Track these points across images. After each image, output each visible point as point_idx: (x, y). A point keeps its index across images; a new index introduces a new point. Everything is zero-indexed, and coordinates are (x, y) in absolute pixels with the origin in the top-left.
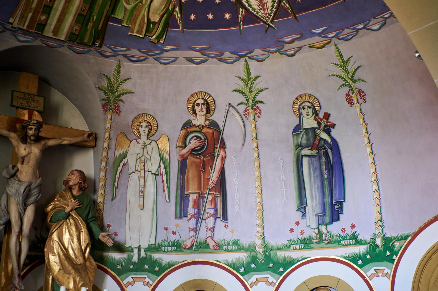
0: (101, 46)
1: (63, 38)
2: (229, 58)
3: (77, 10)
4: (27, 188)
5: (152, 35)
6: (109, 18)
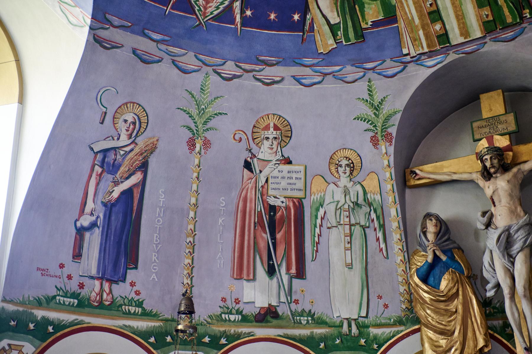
1: (479, 34)
4: (503, 235)
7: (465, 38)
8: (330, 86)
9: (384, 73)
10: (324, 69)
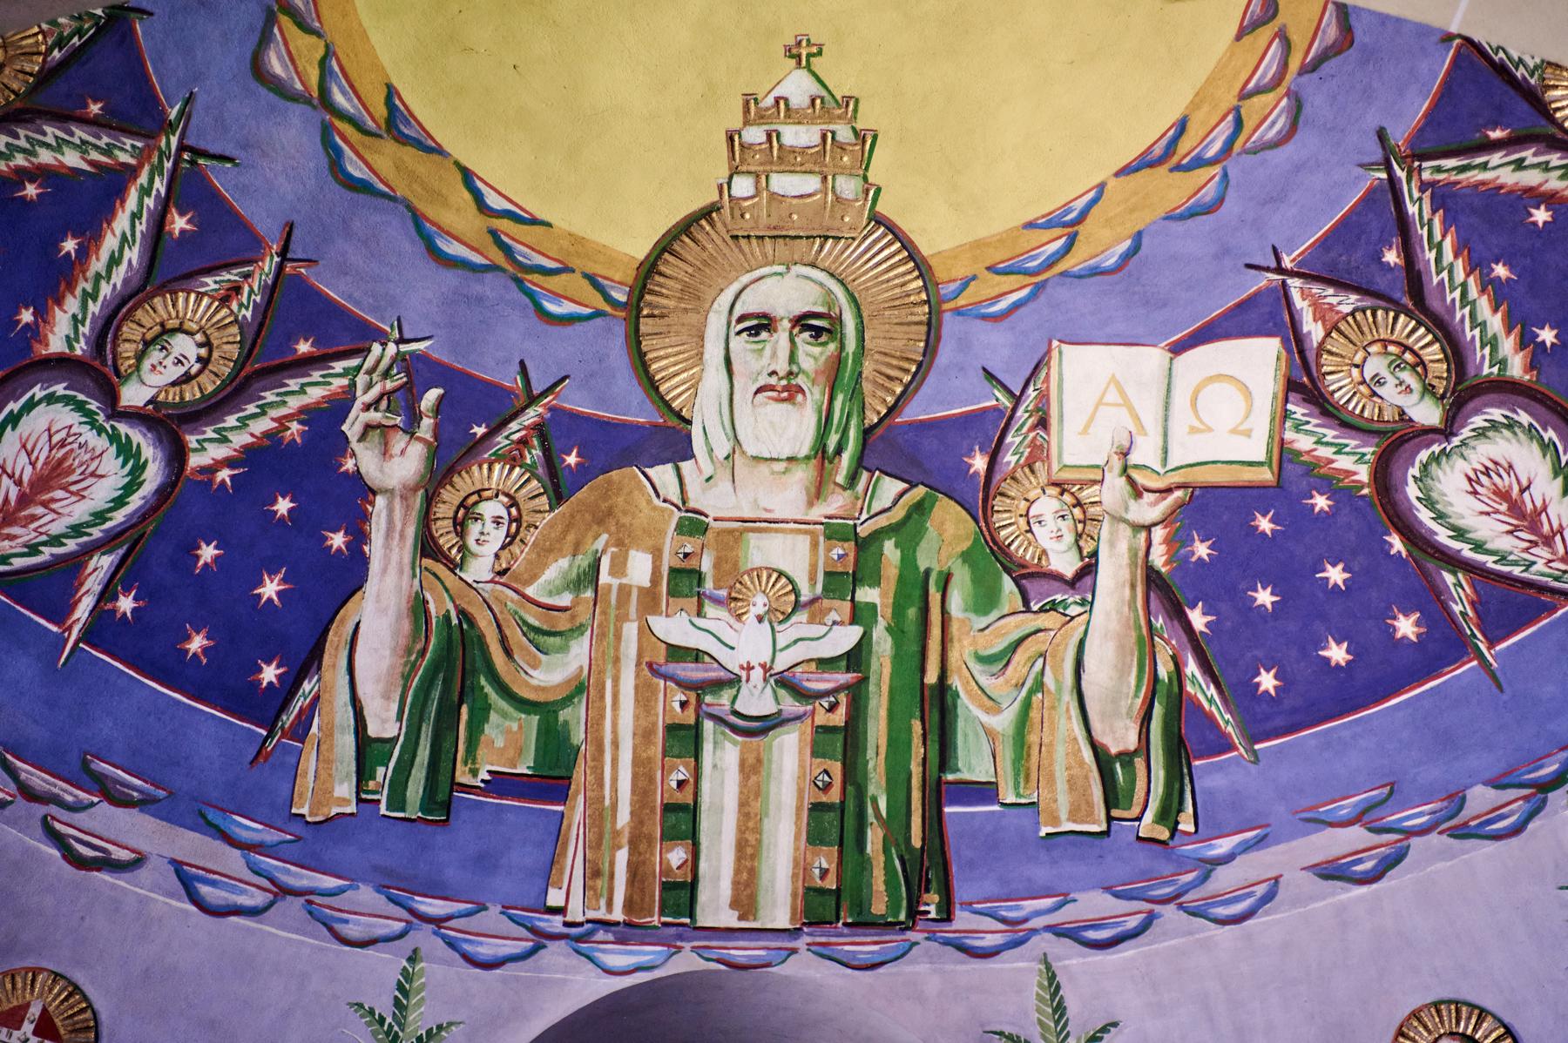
0: (947, 915)
1: (782, 920)
2: (1496, 813)
3: (800, 791)
5: (1135, 811)
6: (938, 793)
7: (741, 918)
8: (284, 937)
9: (467, 947)
10: (288, 872)
